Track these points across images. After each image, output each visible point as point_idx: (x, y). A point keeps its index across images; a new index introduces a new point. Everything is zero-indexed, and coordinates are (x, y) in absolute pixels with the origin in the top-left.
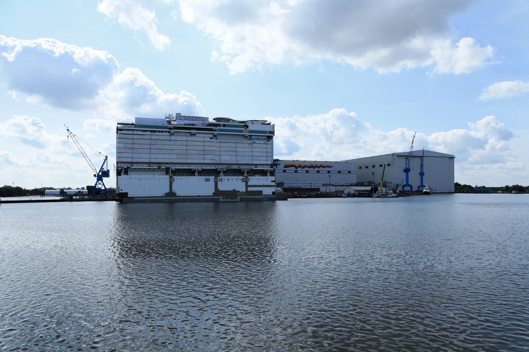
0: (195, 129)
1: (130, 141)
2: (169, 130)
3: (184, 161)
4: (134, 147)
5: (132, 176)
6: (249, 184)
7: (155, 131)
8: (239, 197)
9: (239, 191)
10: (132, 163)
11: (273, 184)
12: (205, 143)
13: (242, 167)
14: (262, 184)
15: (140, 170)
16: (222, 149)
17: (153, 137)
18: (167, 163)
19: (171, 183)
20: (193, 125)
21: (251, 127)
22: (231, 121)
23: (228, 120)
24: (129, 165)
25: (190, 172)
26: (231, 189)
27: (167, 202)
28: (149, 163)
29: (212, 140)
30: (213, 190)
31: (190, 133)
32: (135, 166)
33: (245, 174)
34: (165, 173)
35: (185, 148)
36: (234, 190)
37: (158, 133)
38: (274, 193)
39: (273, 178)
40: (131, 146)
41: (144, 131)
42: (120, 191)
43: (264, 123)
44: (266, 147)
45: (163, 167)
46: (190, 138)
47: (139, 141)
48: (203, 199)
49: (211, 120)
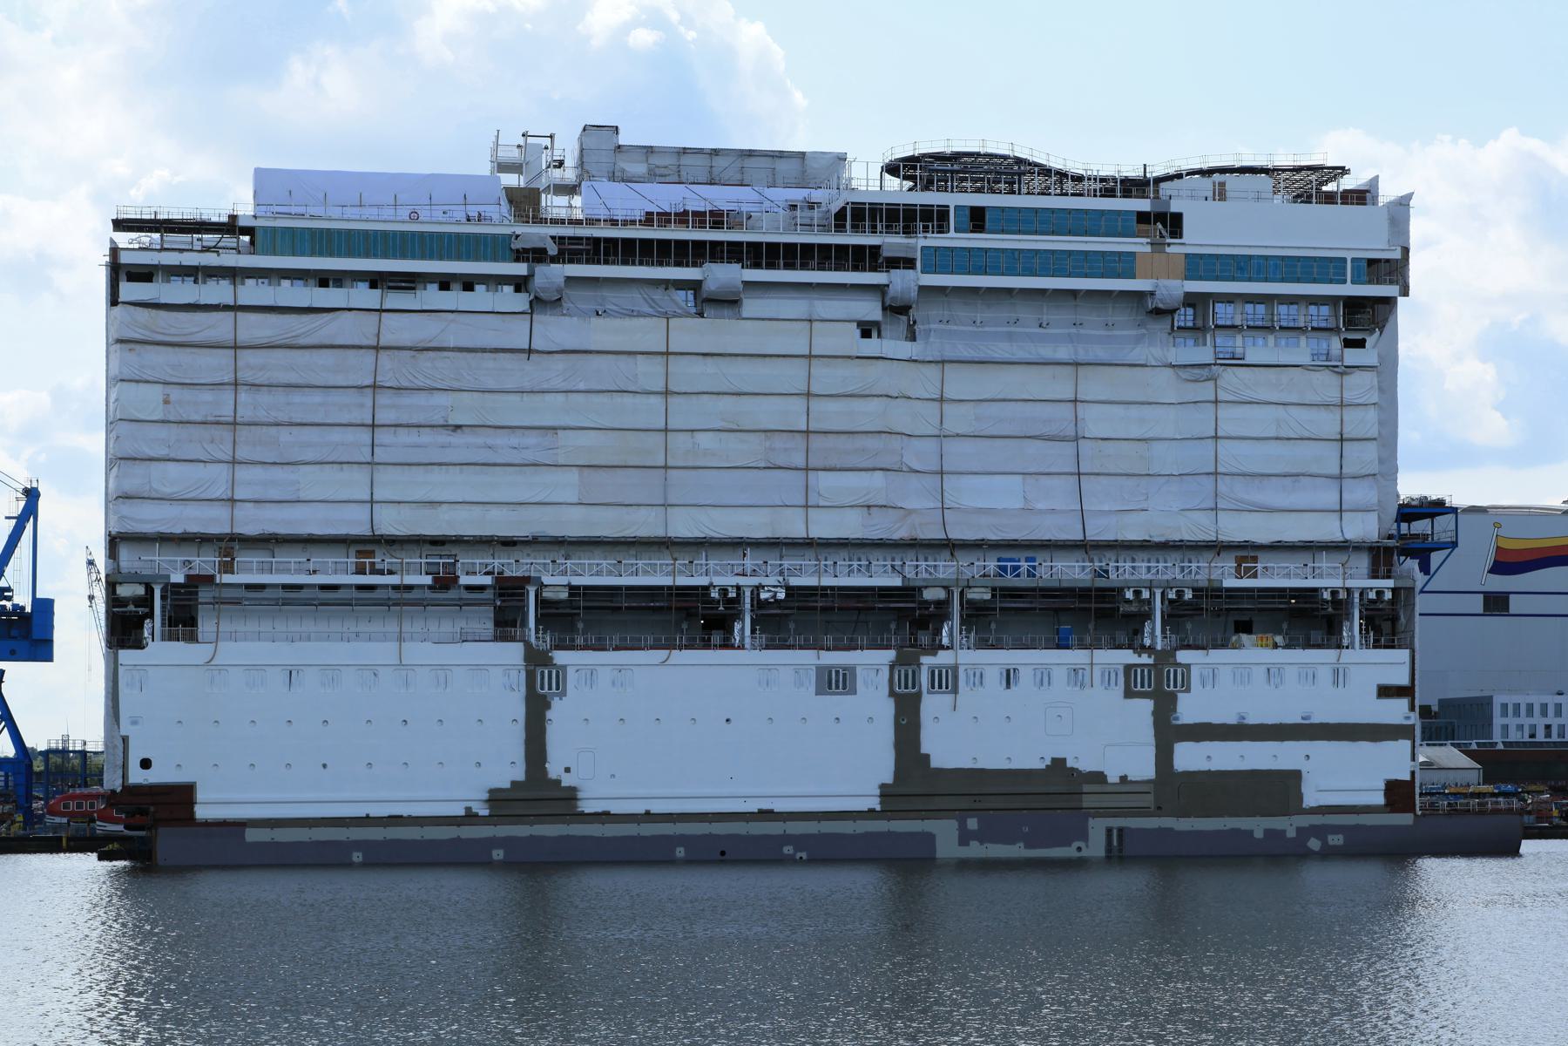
0: (735, 253)
1: (215, 365)
2: (521, 269)
3: (645, 524)
4: (245, 414)
5: (230, 652)
6: (1189, 710)
7: (409, 281)
8: (1097, 828)
9: (1099, 777)
10: (229, 544)
11: (1396, 711)
12: (818, 369)
13: (1126, 572)
14: (1294, 718)
15: (292, 597)
16: (957, 419)
17: (397, 330)
18: (509, 543)
19: (537, 710)
20: (717, 219)
21: (1208, 229)
22: (1037, 182)
23: (1010, 171)
24: (205, 562)
25: (690, 614)
26: (1033, 760)
27: (507, 866)
28: (366, 545)
29: (872, 346)
30: (885, 770)
31: (695, 286)
32: (250, 570)
33: (1154, 633)
34: (488, 626)
35: (649, 411)
36: (1059, 763)
37: (431, 296)
38: (1398, 794)
39: (1392, 665)
40: (223, 404)
41: (324, 279)
42: (137, 776)
43: (1312, 185)
44: (1333, 395)
45: (474, 572)
46: (692, 332)
47: (278, 365)
48: (799, 841)
49: (866, 178)
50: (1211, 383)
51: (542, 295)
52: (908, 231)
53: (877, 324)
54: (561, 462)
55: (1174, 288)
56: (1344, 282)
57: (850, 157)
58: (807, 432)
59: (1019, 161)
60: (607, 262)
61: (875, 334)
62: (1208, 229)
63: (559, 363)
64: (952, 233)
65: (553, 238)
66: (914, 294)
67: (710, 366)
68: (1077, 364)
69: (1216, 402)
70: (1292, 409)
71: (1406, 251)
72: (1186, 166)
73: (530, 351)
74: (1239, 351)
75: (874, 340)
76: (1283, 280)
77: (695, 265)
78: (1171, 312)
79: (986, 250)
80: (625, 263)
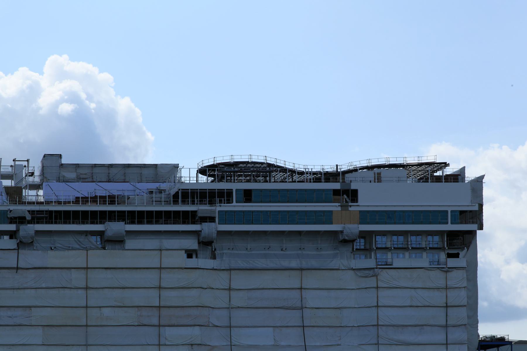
0: (121, 216)
2: (12, 227)
12: (165, 275)
16: (238, 299)
21: (370, 198)
22: (279, 176)
23: (265, 170)
29: (193, 262)
31: (101, 234)
35: (78, 298)
43: (429, 173)
44: (441, 283)
46: (100, 257)
49: (189, 175)
50: (374, 279)
51: (23, 240)
52: (211, 203)
53: (195, 251)
54: (33, 324)
55: (355, 228)
56: (447, 223)
57: (180, 166)
58: (159, 307)
59: (270, 165)
60: (56, 223)
61: (194, 256)
62: (370, 198)
63: (32, 274)
64: (234, 203)
65: (29, 211)
66: (215, 235)
67: (109, 274)
68: (302, 269)
69: (377, 288)
70: (419, 291)
71: (481, 206)
72: (359, 165)
73: (17, 268)
74: (389, 261)
75: (194, 259)
76: (413, 223)
77: (101, 223)
78: (353, 241)
79: (253, 212)
80: (65, 223)
